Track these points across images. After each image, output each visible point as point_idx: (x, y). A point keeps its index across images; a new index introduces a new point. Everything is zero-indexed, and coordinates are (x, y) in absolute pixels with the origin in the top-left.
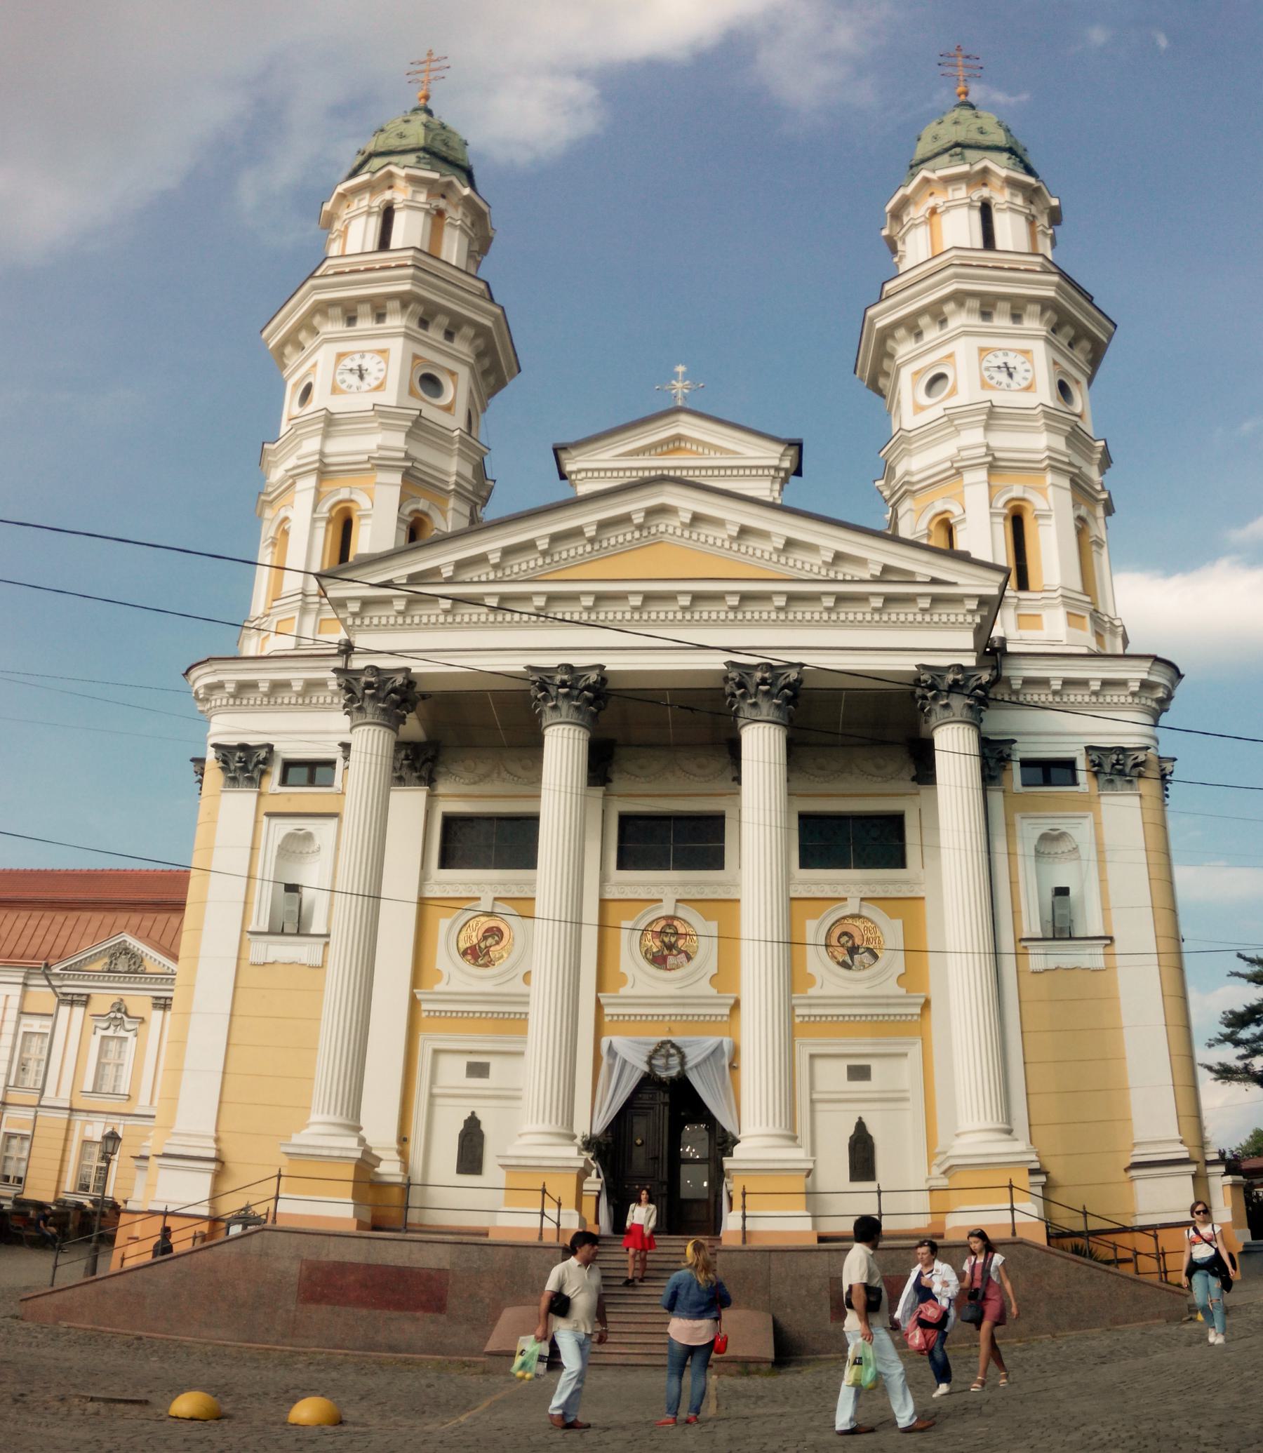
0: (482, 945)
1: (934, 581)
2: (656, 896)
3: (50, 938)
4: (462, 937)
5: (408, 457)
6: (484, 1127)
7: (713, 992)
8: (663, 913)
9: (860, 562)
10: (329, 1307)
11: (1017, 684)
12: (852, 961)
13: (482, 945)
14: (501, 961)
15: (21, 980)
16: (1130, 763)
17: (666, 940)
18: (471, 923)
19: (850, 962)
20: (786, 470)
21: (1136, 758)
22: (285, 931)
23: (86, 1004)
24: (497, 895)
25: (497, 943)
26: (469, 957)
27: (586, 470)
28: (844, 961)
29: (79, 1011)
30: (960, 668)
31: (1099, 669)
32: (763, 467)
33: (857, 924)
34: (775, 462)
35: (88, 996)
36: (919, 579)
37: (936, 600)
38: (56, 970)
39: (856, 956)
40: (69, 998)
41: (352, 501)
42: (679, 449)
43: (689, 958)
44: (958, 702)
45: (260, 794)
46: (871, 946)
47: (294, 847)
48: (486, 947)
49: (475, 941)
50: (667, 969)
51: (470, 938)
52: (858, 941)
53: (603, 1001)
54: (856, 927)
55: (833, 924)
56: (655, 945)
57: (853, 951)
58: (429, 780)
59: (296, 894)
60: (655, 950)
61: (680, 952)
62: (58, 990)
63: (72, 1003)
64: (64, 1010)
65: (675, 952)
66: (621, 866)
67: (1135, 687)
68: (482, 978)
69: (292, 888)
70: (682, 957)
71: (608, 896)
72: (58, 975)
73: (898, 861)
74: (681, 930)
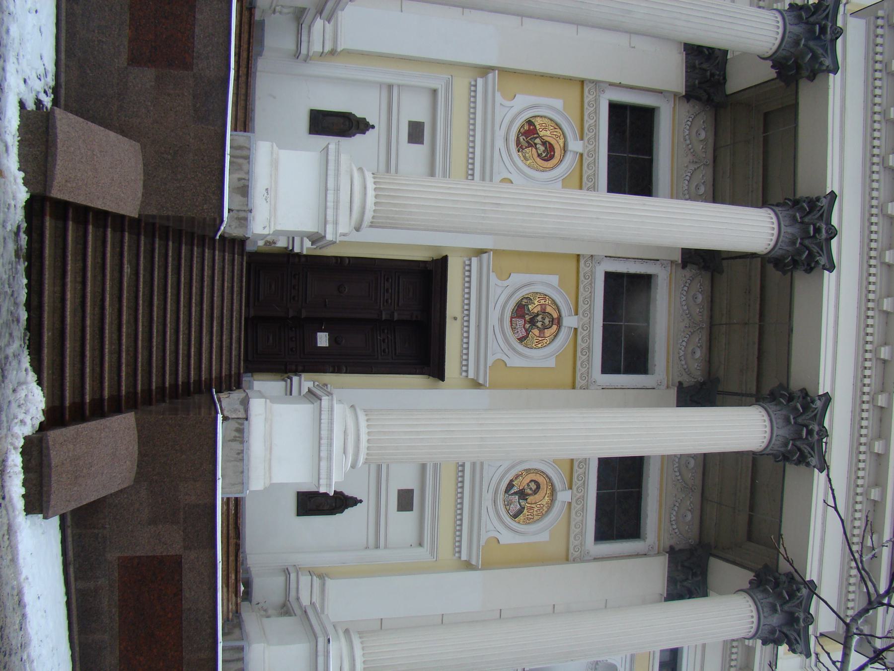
0: (538, 141)
2: (580, 312)
4: (546, 121)
6: (359, 137)
7: (491, 360)
8: (564, 312)
12: (512, 494)
13: (538, 141)
14: (522, 159)
17: (539, 318)
18: (558, 130)
19: (512, 491)
24: (585, 156)
25: (539, 155)
26: (526, 127)
28: (513, 486)
43: (521, 340)
46: (525, 511)
48: (536, 144)
49: (541, 134)
50: (512, 318)
51: (545, 129)
52: (530, 499)
53: (485, 256)
54: (542, 498)
56: (535, 308)
57: (522, 495)
58: (690, 95)
61: (528, 331)
65: (527, 326)
68: (507, 140)
74: (548, 332)
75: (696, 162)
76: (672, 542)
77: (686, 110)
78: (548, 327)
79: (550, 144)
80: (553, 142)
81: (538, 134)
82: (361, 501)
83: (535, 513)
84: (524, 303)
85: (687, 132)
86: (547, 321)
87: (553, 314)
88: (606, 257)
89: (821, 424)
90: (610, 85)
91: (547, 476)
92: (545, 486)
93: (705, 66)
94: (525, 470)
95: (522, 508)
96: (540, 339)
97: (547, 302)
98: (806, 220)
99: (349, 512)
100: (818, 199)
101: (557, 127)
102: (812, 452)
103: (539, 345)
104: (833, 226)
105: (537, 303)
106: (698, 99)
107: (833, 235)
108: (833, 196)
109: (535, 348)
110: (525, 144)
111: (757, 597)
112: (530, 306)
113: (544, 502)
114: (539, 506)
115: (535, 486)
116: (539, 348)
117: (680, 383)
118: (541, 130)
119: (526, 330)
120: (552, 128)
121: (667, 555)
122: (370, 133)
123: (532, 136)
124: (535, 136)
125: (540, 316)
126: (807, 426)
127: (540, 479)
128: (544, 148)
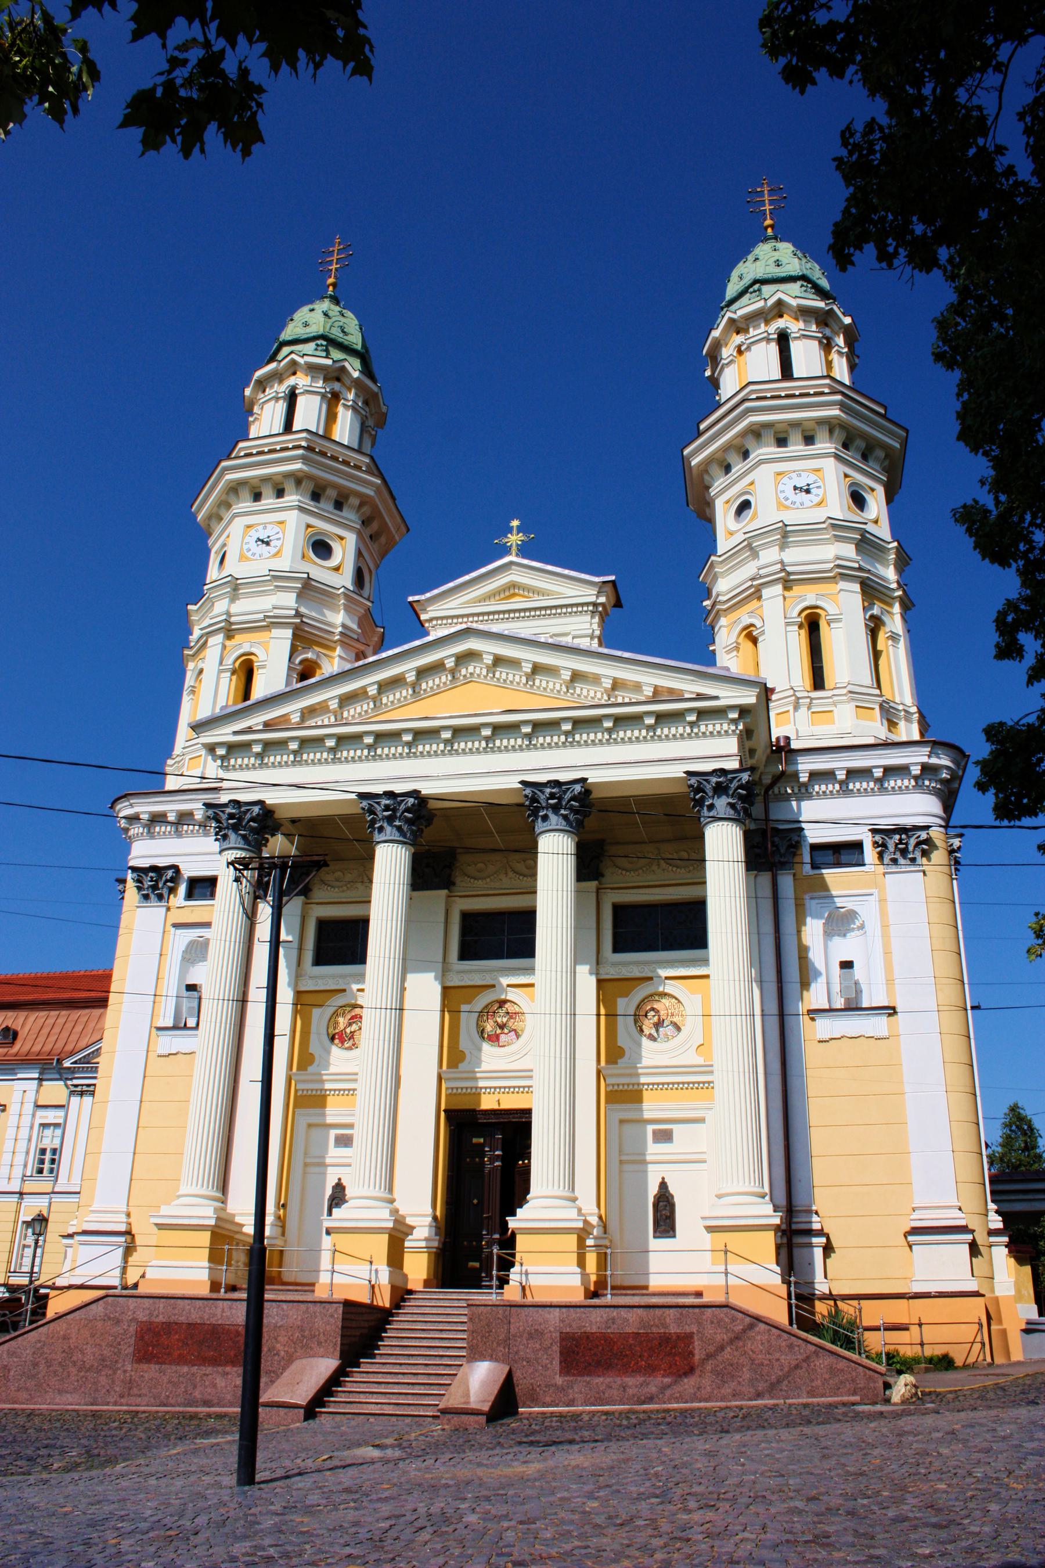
1: (700, 697)
3: (65, 1034)
4: (331, 1024)
5: (298, 614)
9: (638, 687)
10: (157, 1367)
11: (804, 778)
13: (348, 1030)
15: (36, 1076)
16: (913, 842)
17: (499, 1020)
19: (655, 1034)
20: (603, 604)
22: (188, 1025)
23: (92, 1093)
27: (437, 618)
29: (87, 1100)
30: (723, 772)
31: (880, 757)
32: (582, 605)
34: (593, 599)
35: (95, 1085)
36: (687, 696)
37: (702, 714)
38: (67, 1064)
39: (661, 1029)
40: (79, 1089)
41: (252, 654)
42: (514, 595)
43: (518, 1036)
44: (722, 803)
45: (168, 909)
47: (197, 952)
55: (643, 1001)
58: (306, 892)
62: (69, 1083)
63: (82, 1094)
64: (75, 1100)
65: (506, 1031)
67: (916, 770)
69: (192, 988)
72: (69, 1068)
77: (319, 894)
82: (663, 1178)
99: (672, 1189)
110: (351, 1041)
122: (344, 1182)
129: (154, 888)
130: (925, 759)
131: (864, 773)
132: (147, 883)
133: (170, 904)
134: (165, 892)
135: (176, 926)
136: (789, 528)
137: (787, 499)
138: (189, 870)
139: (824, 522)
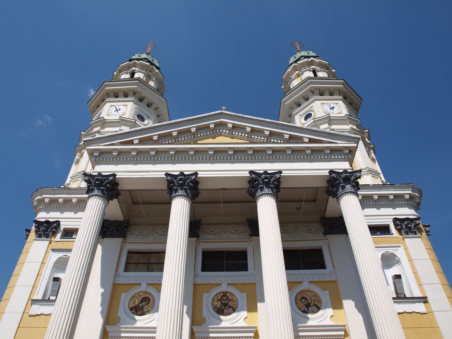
0: (140, 305)
4: (131, 301)
12: (308, 310)
13: (140, 305)
17: (223, 302)
19: (307, 310)
21: (416, 222)
24: (148, 283)
25: (147, 304)
26: (134, 311)
33: (308, 293)
39: (309, 308)
45: (50, 243)
46: (315, 303)
49: (137, 303)
52: (309, 301)
53: (194, 330)
56: (218, 304)
57: (308, 305)
58: (124, 236)
59: (58, 282)
60: (218, 306)
65: (227, 307)
66: (203, 270)
69: (56, 280)
70: (231, 308)
71: (197, 282)
73: (322, 266)
74: (230, 298)
75: (153, 233)
76: (322, 234)
77: (130, 238)
78: (227, 297)
79: (142, 300)
80: (141, 298)
81: (137, 305)
83: (316, 299)
84: (217, 310)
85: (140, 237)
86: (225, 298)
87: (221, 296)
88: (194, 272)
89: (262, 174)
90: (117, 272)
91: (298, 294)
92: (303, 294)
93: (111, 230)
94: (296, 304)
95: (315, 305)
96: (233, 301)
97: (216, 298)
98: (177, 185)
100: (168, 180)
101: (134, 296)
102: (274, 177)
103: (236, 301)
104: (179, 174)
105: (217, 303)
106: (125, 232)
107: (183, 174)
108: (167, 174)
109: (238, 303)
110: (141, 312)
111: (339, 194)
112: (218, 307)
113: (310, 294)
114: (312, 297)
115: (303, 299)
116: (237, 301)
117: (250, 235)
118: (135, 304)
119: (229, 308)
120: (135, 298)
121: (327, 235)
123: (138, 308)
124: (138, 306)
125: (223, 301)
126: (263, 179)
127: (300, 297)
128: (144, 302)
129: (44, 231)
130: (411, 192)
131: (385, 197)
132: (42, 228)
133: (52, 240)
134: (51, 234)
135: (53, 250)
136: (331, 118)
137: (327, 111)
138: (64, 225)
139: (344, 117)
